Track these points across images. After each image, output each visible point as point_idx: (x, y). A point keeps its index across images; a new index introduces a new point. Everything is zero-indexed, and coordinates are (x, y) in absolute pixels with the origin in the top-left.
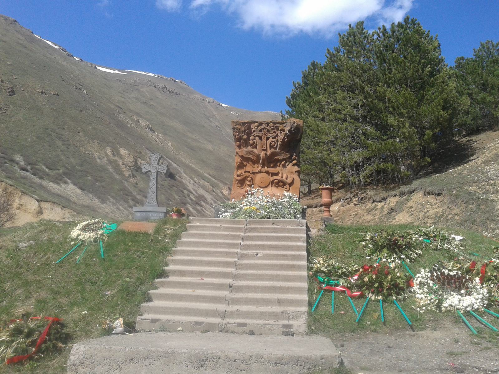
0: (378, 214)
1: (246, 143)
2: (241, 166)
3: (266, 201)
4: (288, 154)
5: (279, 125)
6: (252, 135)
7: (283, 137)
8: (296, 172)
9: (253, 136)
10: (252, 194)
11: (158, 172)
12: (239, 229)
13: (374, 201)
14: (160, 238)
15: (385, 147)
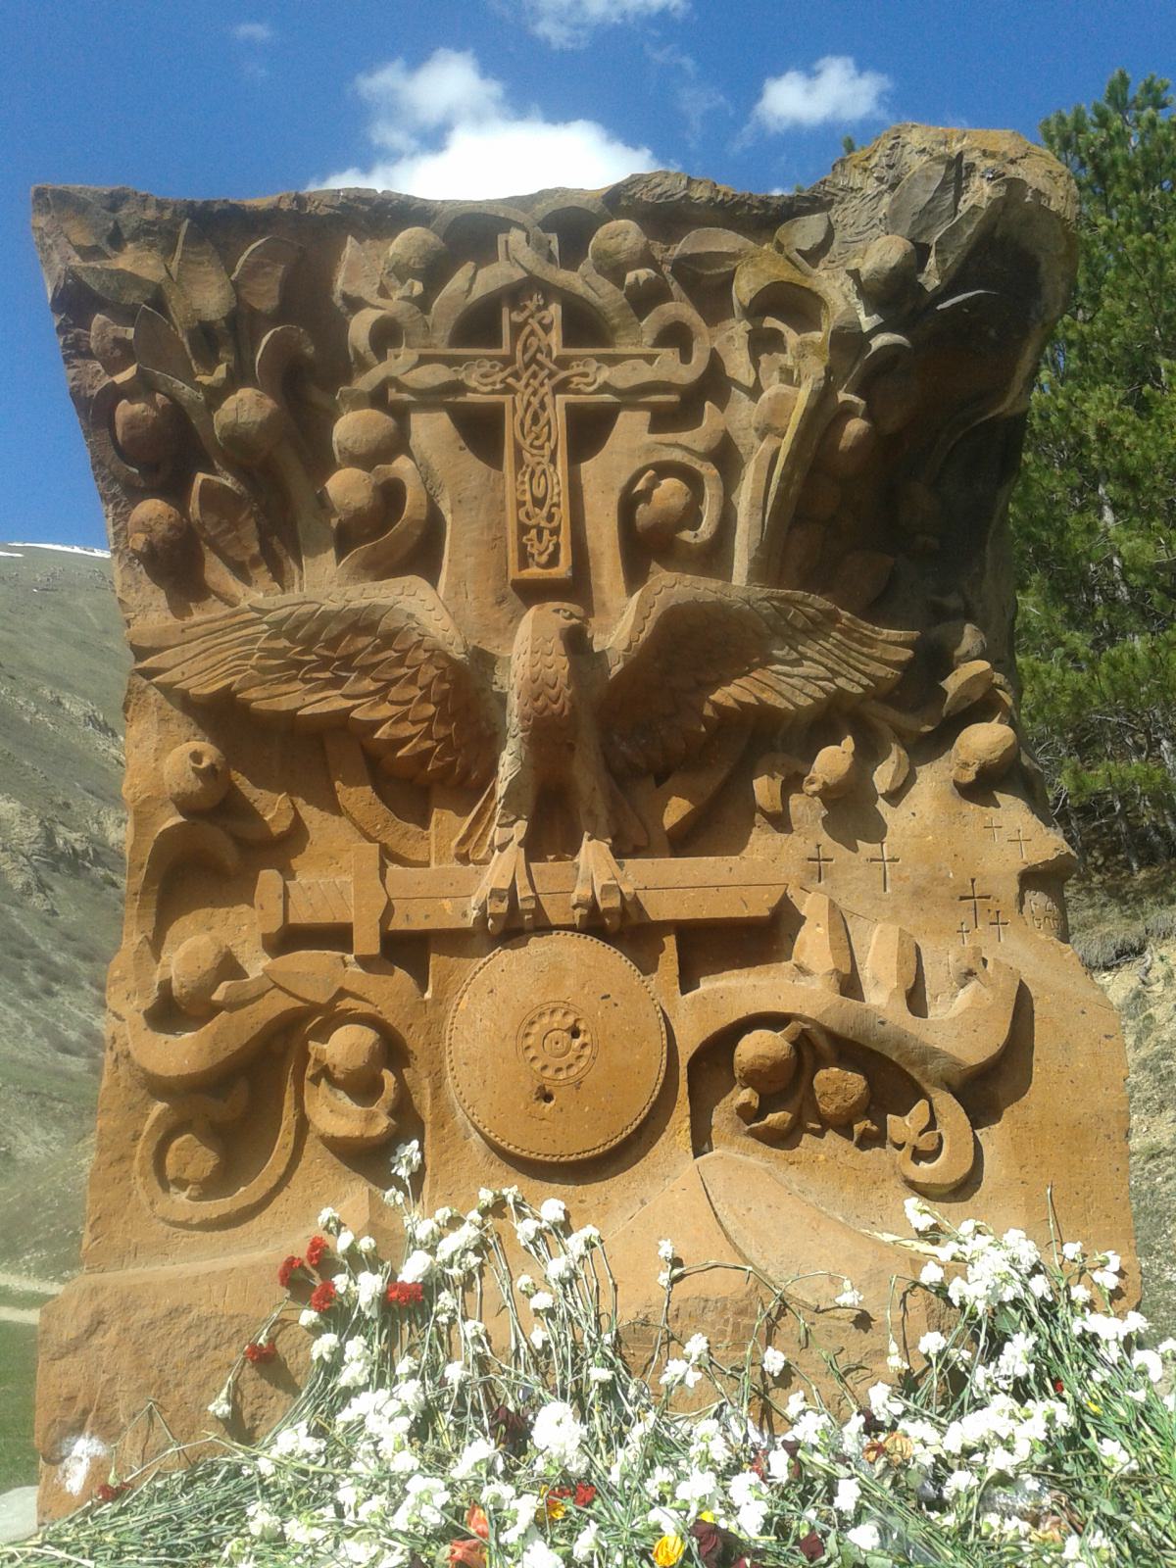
2: (207, 855)
5: (726, 241)
6: (364, 383)
7: (803, 396)
8: (1032, 878)
9: (378, 398)
15: (1113, 682)
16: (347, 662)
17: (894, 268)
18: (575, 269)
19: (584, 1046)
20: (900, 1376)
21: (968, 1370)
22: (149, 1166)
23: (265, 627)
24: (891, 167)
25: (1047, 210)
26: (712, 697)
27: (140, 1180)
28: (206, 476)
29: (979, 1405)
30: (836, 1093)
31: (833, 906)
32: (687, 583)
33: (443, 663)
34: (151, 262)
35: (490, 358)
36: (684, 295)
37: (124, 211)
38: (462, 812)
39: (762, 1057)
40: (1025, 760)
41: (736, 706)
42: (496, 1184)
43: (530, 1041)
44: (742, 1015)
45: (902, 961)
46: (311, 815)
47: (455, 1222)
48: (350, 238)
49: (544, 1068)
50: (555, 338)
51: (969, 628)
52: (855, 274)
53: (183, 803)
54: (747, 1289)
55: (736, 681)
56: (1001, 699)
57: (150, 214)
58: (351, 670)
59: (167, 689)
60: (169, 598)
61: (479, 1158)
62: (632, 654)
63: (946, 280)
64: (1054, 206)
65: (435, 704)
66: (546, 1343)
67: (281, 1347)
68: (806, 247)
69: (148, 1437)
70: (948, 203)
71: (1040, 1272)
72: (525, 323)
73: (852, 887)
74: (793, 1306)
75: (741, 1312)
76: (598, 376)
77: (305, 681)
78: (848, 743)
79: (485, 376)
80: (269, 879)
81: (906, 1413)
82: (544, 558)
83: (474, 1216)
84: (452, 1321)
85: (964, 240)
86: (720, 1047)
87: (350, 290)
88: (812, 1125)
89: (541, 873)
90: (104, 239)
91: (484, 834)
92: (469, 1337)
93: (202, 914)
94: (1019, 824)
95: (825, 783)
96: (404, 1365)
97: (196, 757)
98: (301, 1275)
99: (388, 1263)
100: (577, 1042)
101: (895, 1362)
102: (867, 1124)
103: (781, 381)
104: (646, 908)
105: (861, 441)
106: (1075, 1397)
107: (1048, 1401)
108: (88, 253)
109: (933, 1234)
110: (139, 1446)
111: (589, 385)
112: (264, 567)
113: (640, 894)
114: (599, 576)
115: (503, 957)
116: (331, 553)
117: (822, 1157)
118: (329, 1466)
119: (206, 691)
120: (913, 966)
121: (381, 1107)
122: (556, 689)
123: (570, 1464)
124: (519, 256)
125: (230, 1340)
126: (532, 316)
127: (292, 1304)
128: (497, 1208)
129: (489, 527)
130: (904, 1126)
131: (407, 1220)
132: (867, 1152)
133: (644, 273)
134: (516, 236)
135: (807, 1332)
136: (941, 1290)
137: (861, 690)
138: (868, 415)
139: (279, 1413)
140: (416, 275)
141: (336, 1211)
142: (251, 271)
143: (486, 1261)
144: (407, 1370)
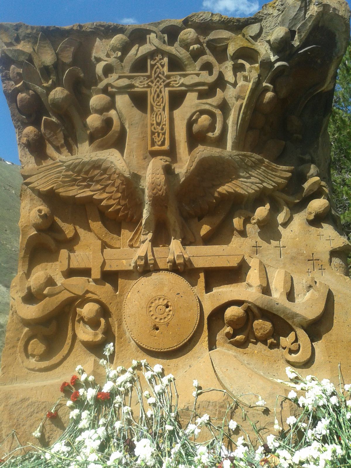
2: (45, 244)
4: (284, 172)
5: (225, 34)
6: (101, 85)
7: (250, 85)
8: (334, 253)
9: (105, 91)
16: (92, 179)
17: (282, 38)
18: (173, 46)
19: (170, 311)
20: (279, 432)
21: (305, 431)
22: (22, 350)
23: (64, 167)
24: (282, 5)
25: (338, 15)
26: (218, 190)
27: (19, 354)
28: (46, 117)
29: (308, 444)
30: (261, 329)
31: (261, 263)
32: (208, 149)
33: (123, 178)
34: (28, 46)
35: (143, 76)
36: (211, 54)
37: (20, 31)
38: (131, 231)
39: (234, 315)
40: (333, 212)
41: (226, 193)
42: (139, 359)
43: (151, 309)
44: (227, 301)
45: (285, 282)
46: (81, 232)
47: (123, 372)
48: (97, 39)
49: (156, 318)
50: (166, 69)
51: (313, 166)
52: (269, 42)
53: (36, 226)
54: (224, 398)
55: (227, 184)
56: (324, 190)
57: (29, 31)
58: (93, 182)
59: (33, 189)
60: (35, 159)
61: (134, 349)
62: (188, 174)
63: (302, 43)
64: (341, 13)
65: (121, 193)
66: (152, 415)
67: (60, 413)
68: (253, 35)
69: (12, 444)
70: (302, 15)
71: (335, 395)
72: (155, 64)
73: (269, 256)
74: (240, 405)
75: (222, 407)
76: (179, 81)
77: (78, 186)
78: (268, 206)
79: (141, 82)
80: (64, 253)
81: (280, 446)
82: (160, 143)
83: (130, 369)
84: (120, 406)
85: (308, 27)
86: (218, 313)
87: (97, 55)
88: (252, 340)
89: (157, 251)
90: (13, 41)
91: (138, 238)
92: (125, 412)
93: (43, 265)
94: (330, 234)
95: (258, 220)
96: (102, 421)
97: (40, 211)
98: (68, 388)
99: (99, 385)
100: (168, 310)
101: (277, 427)
102: (272, 340)
103: (244, 80)
104: (193, 263)
105: (272, 100)
106: (345, 443)
107: (334, 444)
108: (9, 44)
109: (296, 380)
110: (9, 447)
111: (177, 84)
112: (66, 148)
113: (191, 258)
114: (179, 149)
115: (143, 280)
116: (87, 142)
117: (256, 352)
118: (69, 457)
119: (45, 189)
120: (290, 284)
121: (100, 331)
122: (160, 186)
123: (147, 462)
124: (154, 42)
125: (42, 410)
126: (158, 62)
127: (64, 399)
128: (138, 367)
129: (142, 133)
130: (286, 341)
131: (107, 371)
132: (272, 350)
133: (196, 46)
134: (153, 35)
135: (245, 415)
136: (296, 400)
137: (272, 187)
138: (274, 91)
139: (58, 436)
140: (119, 50)
141: (82, 366)
142: (62, 50)
143: (133, 386)
144: (102, 423)
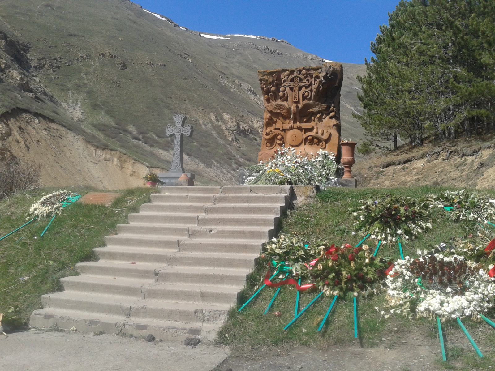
0: (467, 170)
1: (275, 96)
2: (270, 123)
3: (294, 161)
4: (325, 106)
5: (313, 72)
6: (283, 85)
8: (334, 125)
9: (284, 87)
10: (282, 154)
11: (182, 135)
12: (207, 199)
13: (464, 155)
14: (117, 212)
15: (477, 91)
46: (278, 120)
53: (268, 119)
76: (301, 84)
80: (274, 124)
105: (322, 90)
115: (291, 131)
